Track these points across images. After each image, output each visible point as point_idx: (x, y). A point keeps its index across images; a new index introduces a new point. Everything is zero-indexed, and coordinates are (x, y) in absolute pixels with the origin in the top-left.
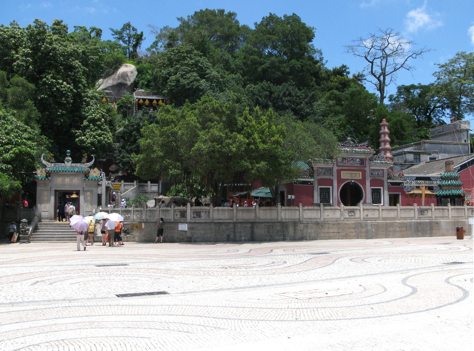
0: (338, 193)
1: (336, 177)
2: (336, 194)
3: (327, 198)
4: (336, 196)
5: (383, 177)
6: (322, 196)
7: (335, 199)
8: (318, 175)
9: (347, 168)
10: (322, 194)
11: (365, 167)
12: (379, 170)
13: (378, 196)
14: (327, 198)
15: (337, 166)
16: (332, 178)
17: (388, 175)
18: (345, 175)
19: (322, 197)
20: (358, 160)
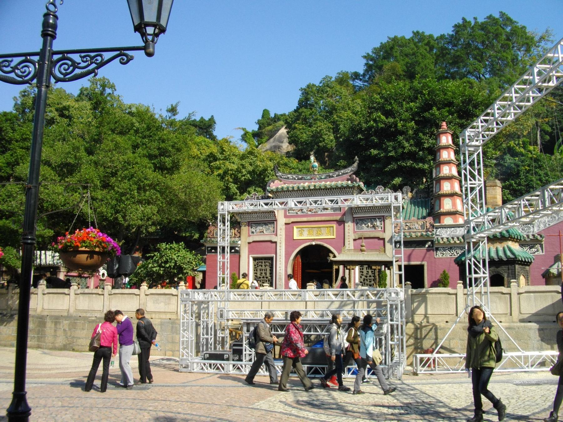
3: (268, 275)
6: (259, 273)
8: (249, 236)
9: (305, 219)
15: (286, 216)
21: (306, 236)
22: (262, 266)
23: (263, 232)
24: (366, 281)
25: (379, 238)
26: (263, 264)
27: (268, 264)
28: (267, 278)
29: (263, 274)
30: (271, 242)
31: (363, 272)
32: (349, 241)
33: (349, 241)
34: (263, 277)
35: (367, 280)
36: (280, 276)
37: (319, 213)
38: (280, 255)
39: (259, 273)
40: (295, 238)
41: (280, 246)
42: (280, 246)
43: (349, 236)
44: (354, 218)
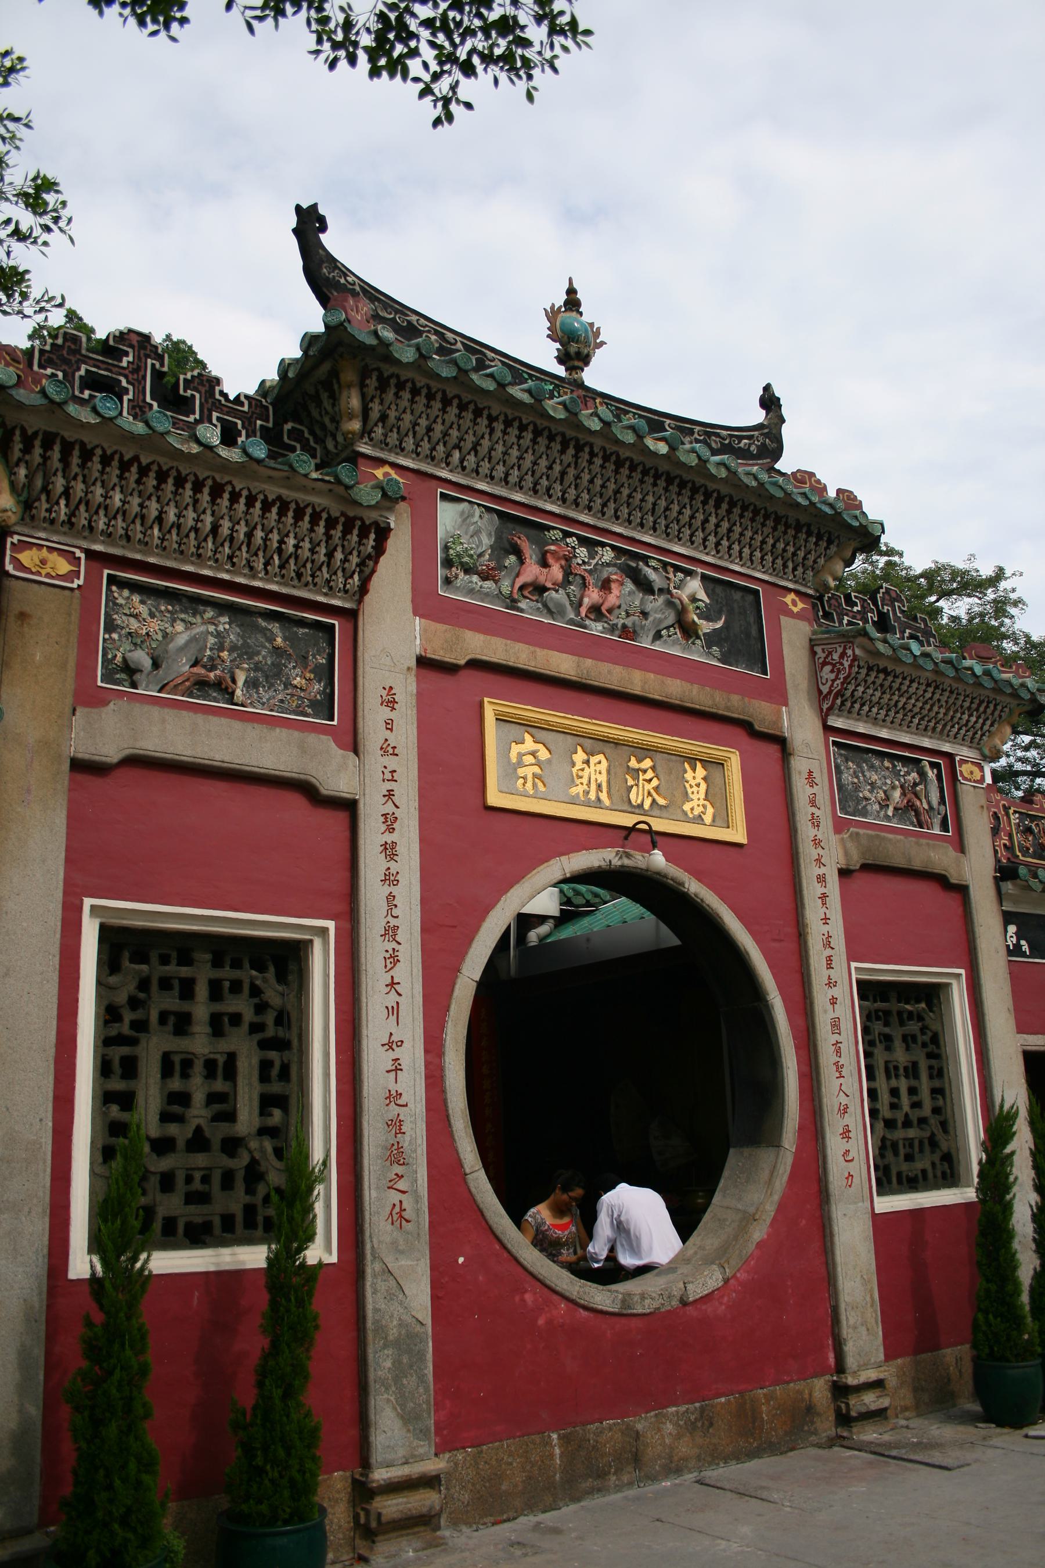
0: (434, 1046)
2: (413, 1054)
4: (413, 1087)
5: (960, 845)
7: (396, 1155)
8: (88, 697)
9: (563, 664)
10: (153, 1048)
11: (777, 693)
12: (909, 758)
13: (925, 1085)
15: (426, 604)
16: (337, 775)
17: (995, 831)
18: (533, 767)
20: (694, 586)
22: (182, 1024)
25: (941, 881)
26: (201, 1010)
28: (232, 1145)
29: (198, 1113)
30: (306, 790)
32: (821, 879)
33: (821, 879)
37: (645, 643)
40: (494, 799)
41: (389, 851)
42: (389, 851)
43: (817, 842)
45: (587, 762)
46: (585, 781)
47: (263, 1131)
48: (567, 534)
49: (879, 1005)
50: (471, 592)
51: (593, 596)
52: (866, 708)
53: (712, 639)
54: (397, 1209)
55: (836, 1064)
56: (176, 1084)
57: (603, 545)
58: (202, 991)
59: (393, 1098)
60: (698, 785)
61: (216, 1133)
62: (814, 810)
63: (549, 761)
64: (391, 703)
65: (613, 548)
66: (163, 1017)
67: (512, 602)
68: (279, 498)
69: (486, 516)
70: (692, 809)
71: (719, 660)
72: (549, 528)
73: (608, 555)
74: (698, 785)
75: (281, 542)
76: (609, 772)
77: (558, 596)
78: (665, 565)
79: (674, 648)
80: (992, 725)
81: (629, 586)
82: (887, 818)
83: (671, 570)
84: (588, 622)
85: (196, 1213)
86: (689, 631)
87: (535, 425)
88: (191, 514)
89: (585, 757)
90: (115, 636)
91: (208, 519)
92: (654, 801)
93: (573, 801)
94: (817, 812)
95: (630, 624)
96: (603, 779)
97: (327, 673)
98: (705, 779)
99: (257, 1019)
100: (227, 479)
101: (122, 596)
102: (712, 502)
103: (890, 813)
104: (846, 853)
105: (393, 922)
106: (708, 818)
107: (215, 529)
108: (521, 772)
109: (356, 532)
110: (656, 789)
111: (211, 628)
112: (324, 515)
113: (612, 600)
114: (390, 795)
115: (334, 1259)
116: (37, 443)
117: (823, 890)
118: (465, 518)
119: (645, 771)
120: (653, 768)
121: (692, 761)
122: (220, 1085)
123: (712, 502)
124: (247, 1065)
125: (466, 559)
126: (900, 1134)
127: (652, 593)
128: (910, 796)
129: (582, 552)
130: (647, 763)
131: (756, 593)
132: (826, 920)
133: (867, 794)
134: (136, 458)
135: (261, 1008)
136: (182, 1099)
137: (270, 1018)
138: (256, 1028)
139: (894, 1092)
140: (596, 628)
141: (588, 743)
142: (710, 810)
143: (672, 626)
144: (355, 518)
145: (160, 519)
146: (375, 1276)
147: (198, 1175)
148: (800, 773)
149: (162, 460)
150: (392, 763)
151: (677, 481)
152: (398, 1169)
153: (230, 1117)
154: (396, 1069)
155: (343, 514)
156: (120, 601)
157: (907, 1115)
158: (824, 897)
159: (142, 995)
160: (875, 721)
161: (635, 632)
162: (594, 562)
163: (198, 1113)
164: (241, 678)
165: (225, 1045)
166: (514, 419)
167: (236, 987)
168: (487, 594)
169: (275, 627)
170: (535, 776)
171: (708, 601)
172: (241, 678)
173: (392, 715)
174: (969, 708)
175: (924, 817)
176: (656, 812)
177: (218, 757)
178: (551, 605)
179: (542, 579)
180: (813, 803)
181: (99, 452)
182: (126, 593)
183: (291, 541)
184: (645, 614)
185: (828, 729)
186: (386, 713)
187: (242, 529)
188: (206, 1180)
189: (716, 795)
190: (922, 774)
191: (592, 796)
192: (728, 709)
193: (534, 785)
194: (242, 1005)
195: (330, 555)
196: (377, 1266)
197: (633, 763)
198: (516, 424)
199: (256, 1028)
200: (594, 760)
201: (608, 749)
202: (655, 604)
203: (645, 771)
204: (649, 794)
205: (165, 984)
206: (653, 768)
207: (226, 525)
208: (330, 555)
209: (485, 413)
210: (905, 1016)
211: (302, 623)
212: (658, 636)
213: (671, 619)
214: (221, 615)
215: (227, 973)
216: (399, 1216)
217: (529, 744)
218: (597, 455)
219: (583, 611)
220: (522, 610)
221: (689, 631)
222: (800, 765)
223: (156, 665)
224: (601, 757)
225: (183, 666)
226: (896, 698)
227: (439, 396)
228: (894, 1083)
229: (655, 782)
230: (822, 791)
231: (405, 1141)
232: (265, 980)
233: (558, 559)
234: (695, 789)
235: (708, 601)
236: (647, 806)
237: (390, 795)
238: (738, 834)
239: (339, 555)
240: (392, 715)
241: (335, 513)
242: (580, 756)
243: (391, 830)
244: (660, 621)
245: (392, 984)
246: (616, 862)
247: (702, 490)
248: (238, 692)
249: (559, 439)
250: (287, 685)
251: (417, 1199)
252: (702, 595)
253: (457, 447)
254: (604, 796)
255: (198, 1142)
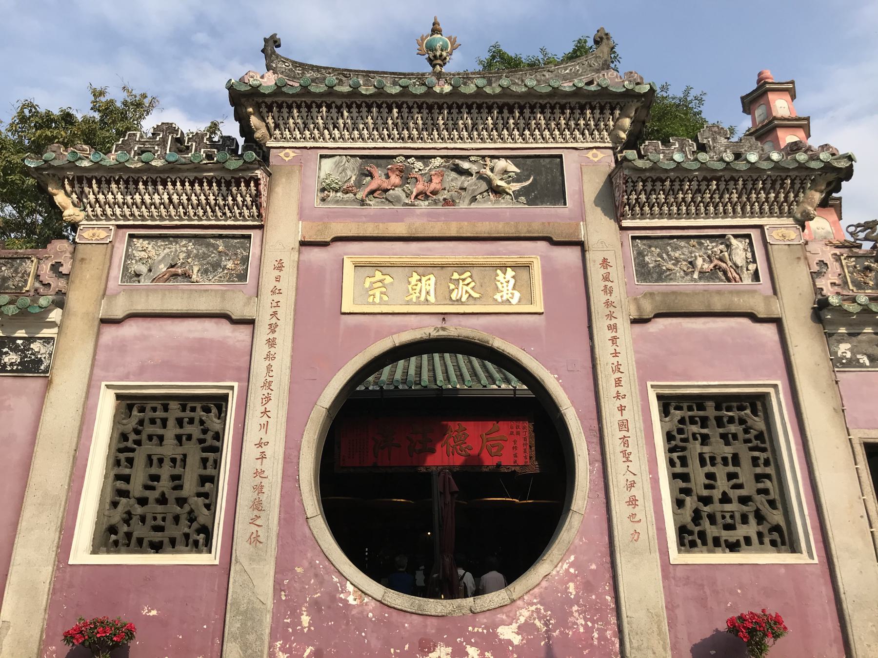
1: (287, 301)
2: (276, 449)
3: (190, 486)
4: (274, 469)
6: (139, 476)
7: (257, 505)
9: (399, 229)
14: (190, 486)
19: (136, 487)
21: (397, 297)
23: (186, 276)
24: (706, 524)
26: (170, 432)
27: (194, 430)
29: (164, 485)
31: (685, 477)
32: (613, 328)
33: (613, 328)
34: (162, 500)
35: (712, 518)
36: (259, 489)
38: (268, 385)
39: (139, 476)
42: (271, 343)
43: (608, 304)
44: (622, 228)
45: (420, 280)
46: (417, 291)
47: (199, 495)
48: (407, 157)
49: (695, 413)
50: (337, 202)
51: (420, 186)
52: (656, 209)
53: (517, 194)
54: (254, 535)
55: (623, 452)
56: (154, 470)
57: (435, 157)
58: (171, 423)
59: (258, 473)
60: (508, 282)
61: (171, 496)
62: (607, 283)
63: (392, 284)
64: (280, 267)
65: (442, 157)
66: (150, 438)
67: (362, 202)
68: (196, 178)
69: (352, 160)
70: (502, 297)
71: (528, 204)
72: (394, 157)
73: (438, 161)
74: (508, 282)
75: (207, 199)
76: (436, 284)
77: (398, 192)
78: (483, 157)
79: (489, 204)
80: (796, 196)
81: (453, 175)
82: (695, 280)
83: (488, 159)
84: (416, 203)
85: (157, 537)
86: (498, 191)
87: (366, 103)
88: (156, 196)
89: (419, 277)
90: (134, 261)
91: (166, 197)
92: (470, 295)
93: (408, 303)
94: (609, 284)
95: (448, 197)
96: (432, 289)
97: (245, 260)
98: (513, 277)
99: (202, 436)
100: (167, 175)
101: (139, 243)
102: (505, 111)
103: (696, 276)
104: (639, 308)
105: (269, 379)
106: (514, 301)
107: (170, 200)
108: (371, 293)
109: (243, 184)
110: (473, 288)
111: (184, 249)
112: (223, 181)
113: (434, 185)
114: (275, 313)
115: (217, 562)
116: (76, 182)
117: (614, 334)
118: (337, 165)
119: (464, 280)
120: (471, 277)
121: (504, 267)
122: (178, 471)
123: (505, 111)
124: (194, 460)
125: (334, 185)
126: (716, 507)
127: (472, 175)
128: (716, 262)
129: (419, 165)
130: (468, 274)
131: (560, 157)
132: (616, 354)
133: (671, 266)
134: (120, 177)
135: (205, 431)
136: (156, 478)
137: (209, 436)
138: (201, 441)
139: (710, 476)
140: (424, 204)
141: (420, 270)
142: (517, 295)
143: (486, 191)
144: (240, 178)
145: (143, 202)
146: (236, 572)
147: (159, 517)
148: (594, 261)
149: (133, 175)
150: (277, 298)
151: (475, 106)
152: (256, 512)
153: (180, 487)
154: (263, 457)
155: (232, 178)
156: (138, 245)
157: (724, 494)
158: (614, 340)
159: (140, 428)
160: (670, 216)
161: (453, 201)
162: (428, 168)
163: (164, 485)
164: (196, 269)
165: (180, 450)
166: (352, 103)
167: (191, 421)
168: (347, 201)
169: (219, 242)
170: (382, 293)
171: (519, 171)
172: (196, 269)
173: (280, 274)
174: (763, 188)
175: (732, 273)
176: (471, 301)
177: (175, 308)
178: (389, 198)
179: (385, 185)
180: (606, 278)
181: (103, 179)
182: (141, 240)
183: (212, 197)
184: (464, 189)
185: (622, 228)
186: (277, 273)
187: (184, 197)
188: (164, 519)
189: (524, 286)
190: (729, 246)
191: (422, 298)
192: (529, 232)
193: (381, 298)
194: (194, 430)
195: (234, 199)
196: (238, 567)
197: (456, 276)
198: (354, 106)
199: (201, 441)
200: (424, 279)
201: (436, 271)
202: (467, 182)
203: (464, 280)
204: (467, 292)
205: (153, 421)
206: (471, 277)
207: (175, 197)
208: (234, 199)
209: (333, 105)
210: (725, 420)
211: (234, 237)
212: (474, 199)
213: (484, 186)
214: (190, 241)
215: (188, 414)
216: (255, 540)
217: (378, 275)
218: (412, 107)
219: (413, 197)
220: (370, 205)
221: (498, 191)
222: (594, 257)
223: (150, 270)
224: (432, 276)
225: (163, 268)
226: (681, 196)
227: (303, 105)
228: (709, 468)
229: (473, 284)
230: (616, 272)
231: (263, 498)
232: (207, 417)
233: (393, 172)
234: (505, 284)
235: (519, 171)
236: (464, 299)
237: (275, 313)
238: (538, 306)
239: (239, 199)
240: (280, 274)
241: (228, 178)
242: (416, 277)
243: (274, 331)
244: (474, 191)
245: (265, 412)
246: (434, 334)
247: (495, 106)
248: (194, 277)
249: (384, 105)
250: (224, 268)
251: (268, 529)
252: (512, 168)
253: (325, 128)
254: (432, 299)
255: (162, 500)
